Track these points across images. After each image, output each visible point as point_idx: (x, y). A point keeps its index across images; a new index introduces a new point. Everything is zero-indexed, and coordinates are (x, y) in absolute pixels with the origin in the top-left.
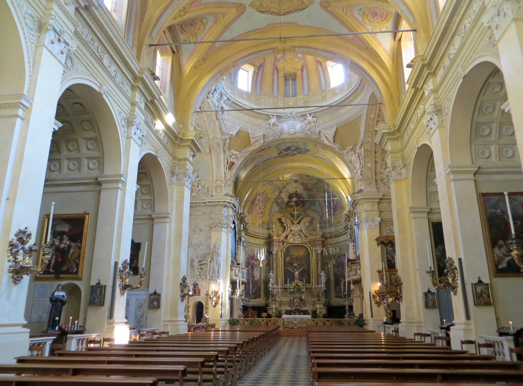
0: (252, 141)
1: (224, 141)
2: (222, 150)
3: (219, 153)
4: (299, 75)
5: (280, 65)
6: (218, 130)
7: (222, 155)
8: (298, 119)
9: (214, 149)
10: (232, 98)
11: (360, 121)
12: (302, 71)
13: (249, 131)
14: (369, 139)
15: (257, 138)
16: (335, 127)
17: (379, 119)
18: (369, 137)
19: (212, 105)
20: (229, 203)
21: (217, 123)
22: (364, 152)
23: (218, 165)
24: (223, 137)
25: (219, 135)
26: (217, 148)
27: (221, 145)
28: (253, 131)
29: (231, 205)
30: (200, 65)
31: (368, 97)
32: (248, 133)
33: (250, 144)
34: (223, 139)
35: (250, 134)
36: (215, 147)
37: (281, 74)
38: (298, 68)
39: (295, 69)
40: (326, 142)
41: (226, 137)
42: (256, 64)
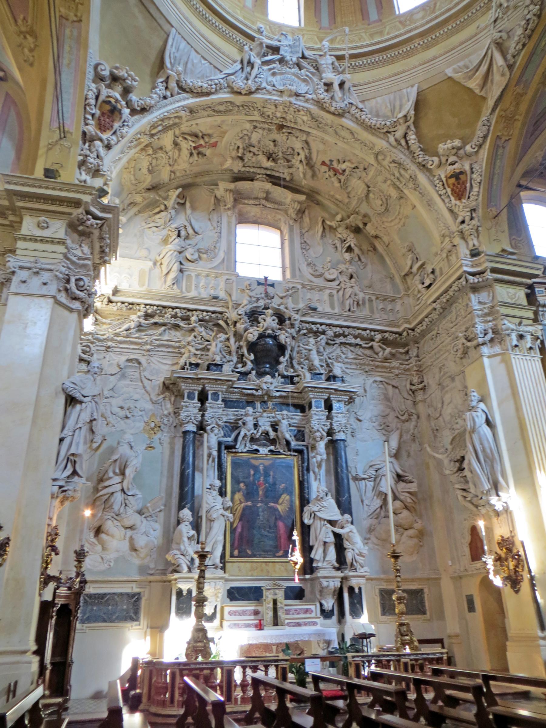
0: (474, 84)
1: (403, 142)
2: (413, 168)
3: (413, 179)
6: (365, 136)
7: (422, 178)
10: (344, 49)
13: (449, 72)
15: (484, 68)
19: (286, 98)
20: (473, 274)
21: (346, 122)
23: (430, 204)
24: (392, 139)
25: (380, 144)
26: (403, 172)
27: (401, 157)
28: (461, 64)
29: (489, 275)
30: (31, 50)
32: (450, 78)
34: (394, 143)
35: (456, 76)
36: (397, 174)
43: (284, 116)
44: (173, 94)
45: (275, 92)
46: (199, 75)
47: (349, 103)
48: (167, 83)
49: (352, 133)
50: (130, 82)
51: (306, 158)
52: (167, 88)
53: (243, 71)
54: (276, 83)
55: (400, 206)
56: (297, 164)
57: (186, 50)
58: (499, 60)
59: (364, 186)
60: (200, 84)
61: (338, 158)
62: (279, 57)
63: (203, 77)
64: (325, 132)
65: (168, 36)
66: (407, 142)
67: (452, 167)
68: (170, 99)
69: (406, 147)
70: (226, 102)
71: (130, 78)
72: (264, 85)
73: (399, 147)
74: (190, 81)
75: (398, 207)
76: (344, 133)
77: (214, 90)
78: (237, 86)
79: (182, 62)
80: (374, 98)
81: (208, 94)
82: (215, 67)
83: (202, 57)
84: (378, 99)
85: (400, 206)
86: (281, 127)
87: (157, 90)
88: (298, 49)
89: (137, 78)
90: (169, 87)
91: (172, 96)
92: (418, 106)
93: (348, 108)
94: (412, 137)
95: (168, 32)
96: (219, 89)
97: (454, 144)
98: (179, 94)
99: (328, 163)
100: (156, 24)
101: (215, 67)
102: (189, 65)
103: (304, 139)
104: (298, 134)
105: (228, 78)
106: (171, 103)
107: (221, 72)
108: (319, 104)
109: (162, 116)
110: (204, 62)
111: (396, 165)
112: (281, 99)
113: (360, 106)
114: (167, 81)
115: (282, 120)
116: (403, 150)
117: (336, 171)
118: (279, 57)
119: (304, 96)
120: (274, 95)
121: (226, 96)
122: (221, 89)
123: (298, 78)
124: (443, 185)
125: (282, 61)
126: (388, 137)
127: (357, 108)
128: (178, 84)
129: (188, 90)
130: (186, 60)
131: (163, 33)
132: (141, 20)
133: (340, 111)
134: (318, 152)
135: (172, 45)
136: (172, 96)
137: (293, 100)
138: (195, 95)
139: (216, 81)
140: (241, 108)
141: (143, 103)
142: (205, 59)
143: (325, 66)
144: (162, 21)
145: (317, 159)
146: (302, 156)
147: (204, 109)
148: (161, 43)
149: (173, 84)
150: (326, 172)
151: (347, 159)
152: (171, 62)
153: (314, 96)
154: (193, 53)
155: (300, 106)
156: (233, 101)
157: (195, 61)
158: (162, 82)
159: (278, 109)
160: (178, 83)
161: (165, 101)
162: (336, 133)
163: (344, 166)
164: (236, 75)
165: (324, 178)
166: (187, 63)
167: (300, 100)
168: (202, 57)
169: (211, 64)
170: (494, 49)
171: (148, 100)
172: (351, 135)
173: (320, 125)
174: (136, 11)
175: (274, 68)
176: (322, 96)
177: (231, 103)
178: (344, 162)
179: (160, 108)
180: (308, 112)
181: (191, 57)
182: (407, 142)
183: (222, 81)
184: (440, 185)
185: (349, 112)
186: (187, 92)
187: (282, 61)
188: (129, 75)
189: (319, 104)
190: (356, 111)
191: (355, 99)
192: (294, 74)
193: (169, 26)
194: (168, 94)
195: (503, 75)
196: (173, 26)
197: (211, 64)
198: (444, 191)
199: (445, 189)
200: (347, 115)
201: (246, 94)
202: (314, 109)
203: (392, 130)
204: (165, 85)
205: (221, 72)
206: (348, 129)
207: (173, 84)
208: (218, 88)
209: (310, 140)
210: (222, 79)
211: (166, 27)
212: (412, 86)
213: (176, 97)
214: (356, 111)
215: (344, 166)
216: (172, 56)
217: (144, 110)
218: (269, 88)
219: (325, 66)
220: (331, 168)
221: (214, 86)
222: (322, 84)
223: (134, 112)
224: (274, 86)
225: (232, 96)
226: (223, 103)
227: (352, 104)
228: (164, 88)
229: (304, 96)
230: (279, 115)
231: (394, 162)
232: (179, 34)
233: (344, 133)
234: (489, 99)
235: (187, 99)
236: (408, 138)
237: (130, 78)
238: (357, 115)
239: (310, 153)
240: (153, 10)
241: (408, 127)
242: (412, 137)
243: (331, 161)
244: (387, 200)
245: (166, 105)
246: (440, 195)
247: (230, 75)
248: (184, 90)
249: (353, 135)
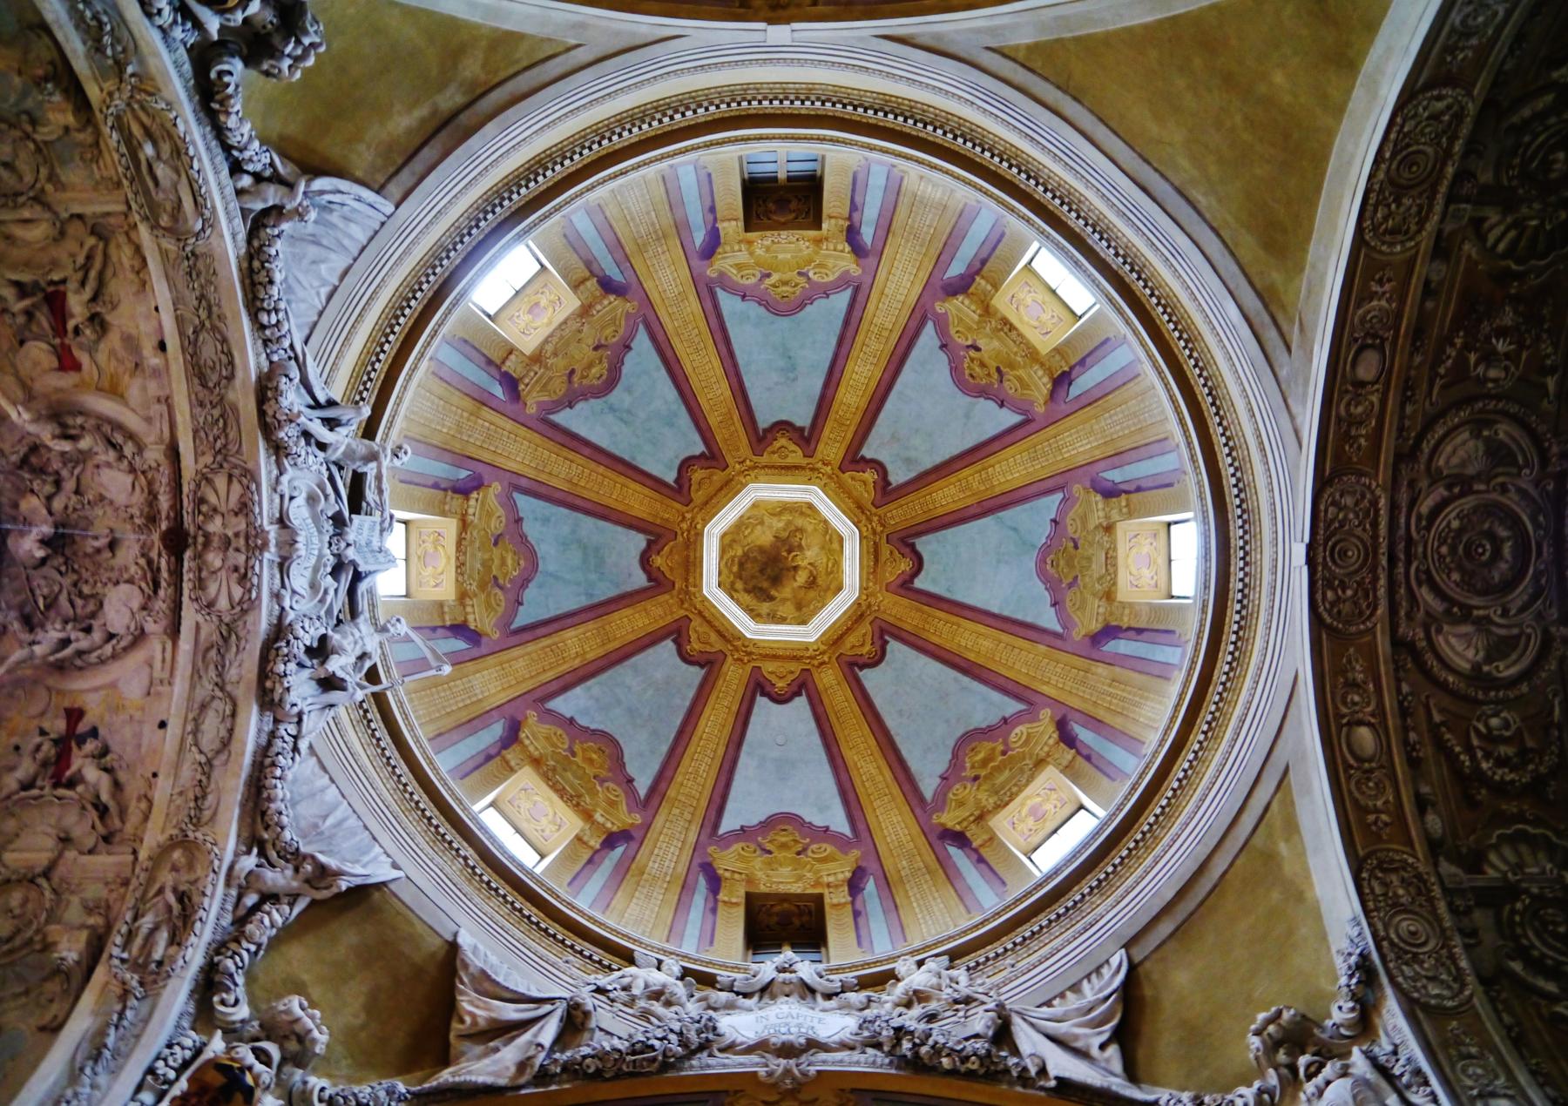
0: (474, 1008)
1: (251, 899)
3: (153, 974)
4: (834, 906)
5: (727, 861)
8: (833, 1003)
9: (130, 936)
11: (1291, 826)
12: (855, 885)
13: (465, 940)
14: (1406, 925)
15: (511, 1012)
16: (1118, 957)
17: (1425, 789)
18: (1397, 907)
19: (272, 531)
22: (1411, 1017)
26: (163, 936)
31: (1299, 552)
33: (446, 1045)
36: (147, 922)
37: (734, 894)
38: (831, 879)
39: (817, 883)
40: (1062, 1065)
41: (279, 877)
42: (598, 817)
43: (216, 542)
44: (246, 198)
45: (277, 500)
46: (291, 280)
47: (300, 715)
48: (269, 180)
49: (225, 744)
50: (288, 50)
51: (80, 653)
52: (258, 178)
53: (310, 407)
54: (295, 503)
55: (27, 993)
56: (53, 634)
57: (346, 242)
58: (548, 1032)
59: (41, 859)
60: (278, 277)
61: (114, 747)
62: (346, 513)
63: (289, 289)
64: (196, 675)
65: (378, 192)
66: (256, 908)
67: (250, 1059)
68: (230, 191)
69: (241, 912)
70: (231, 363)
71: (299, 52)
72: (290, 472)
73: (234, 892)
74: (281, 247)
75: (19, 989)
76: (212, 727)
77: (264, 318)
78: (283, 387)
79: (320, 230)
80: (332, 780)
81: (255, 306)
82: (315, 324)
83: (336, 289)
84: (333, 790)
85: (27, 993)
86: (176, 541)
87: (256, 144)
88: (371, 560)
89: (298, 75)
90: (264, 186)
91: (240, 193)
92: (363, 893)
93: (288, 715)
94: (277, 916)
95: (385, 192)
96: (267, 338)
97: (316, 1034)
98: (245, 212)
99: (82, 728)
100: (400, 161)
101: (315, 324)
102: (313, 251)
103: (150, 627)
104: (161, 605)
105: (293, 362)
106: (221, 189)
107: (306, 342)
108: (280, 631)
109: (191, 152)
110: (324, 291)
111: (176, 907)
112: (265, 522)
113: (303, 745)
114: (276, 179)
115: (201, 540)
116: (229, 907)
117: (63, 758)
118: (346, 513)
119: (283, 586)
120: (271, 501)
121: (252, 360)
122: (266, 342)
123: (316, 570)
124: (186, 1064)
125: (339, 521)
126: (249, 852)
127: (295, 738)
128: (265, 212)
129: (256, 243)
130: (325, 242)
131: (381, 179)
132: (403, 122)
133: (279, 690)
134: (113, 685)
135: (359, 200)
136: (240, 193)
137: (271, 555)
138: (245, 265)
139: (286, 327)
140: (216, 412)
141: (230, 90)
142: (330, 297)
143: (357, 634)
144: (406, 177)
145: (87, 689)
146: (83, 643)
147: (201, 298)
148: (359, 174)
149: (272, 195)
150: (43, 733)
151: (122, 776)
152: (322, 192)
153: (291, 616)
154: (341, 262)
155: (260, 577)
156: (238, 382)
157: (323, 267)
158: (272, 164)
159: (234, 520)
160: (277, 212)
161: (225, 172)
162: (204, 707)
163: (92, 773)
164: (303, 391)
165: (15, 740)
166: (317, 243)
167: (272, 577)
168: (336, 289)
169: (320, 314)
170: (558, 1013)
171: (237, 105)
172: (217, 745)
173: (213, 653)
174: (422, 112)
175: (326, 497)
176: (301, 633)
177: (231, 378)
178: (106, 770)
179: (208, 149)
180: (246, 606)
181: (333, 256)
182: (256, 908)
183: (286, 344)
184: (180, 1055)
185: (276, 721)
186: (249, 242)
187: (339, 521)
188: (306, 51)
189: (280, 631)
190: (287, 738)
191: (314, 725)
192: (320, 556)
193: (398, 196)
194: (246, 181)
195: (522, 1066)
196: (397, 207)
197: (320, 314)
198: (172, 1075)
199: (180, 1071)
200: (269, 717)
201: (262, 413)
202: (263, 621)
203: (273, 855)
204: (268, 173)
205: (306, 342)
206: (231, 731)
207: (272, 195)
208: (268, 332)
209: (155, 647)
210: (292, 346)
211: (395, 189)
212: (395, 866)
213: (234, 205)
214: (287, 738)
215: (92, 773)
216: (336, 198)
217: (209, 96)
218: (285, 479)
219: (357, 634)
220: (65, 745)
221: (274, 321)
222: (323, 631)
223: (203, 57)
224: (292, 498)
225: (254, 377)
226: (229, 354)
227: (300, 722)
228: (259, 167)
229: (283, 586)
230: (215, 526)
231: (182, 897)
232: (383, 224)
233: (212, 727)
234: (451, 1069)
235: (234, 236)
236: (267, 907)
237: (299, 52)
238: (279, 743)
239: (102, 661)
240: (427, 154)
241: (294, 898)
242: (277, 916)
243: (94, 733)
244: (30, 941)
245: (217, 173)
246: (151, 1071)
247: (302, 368)
248: (252, 235)
249: (218, 752)
